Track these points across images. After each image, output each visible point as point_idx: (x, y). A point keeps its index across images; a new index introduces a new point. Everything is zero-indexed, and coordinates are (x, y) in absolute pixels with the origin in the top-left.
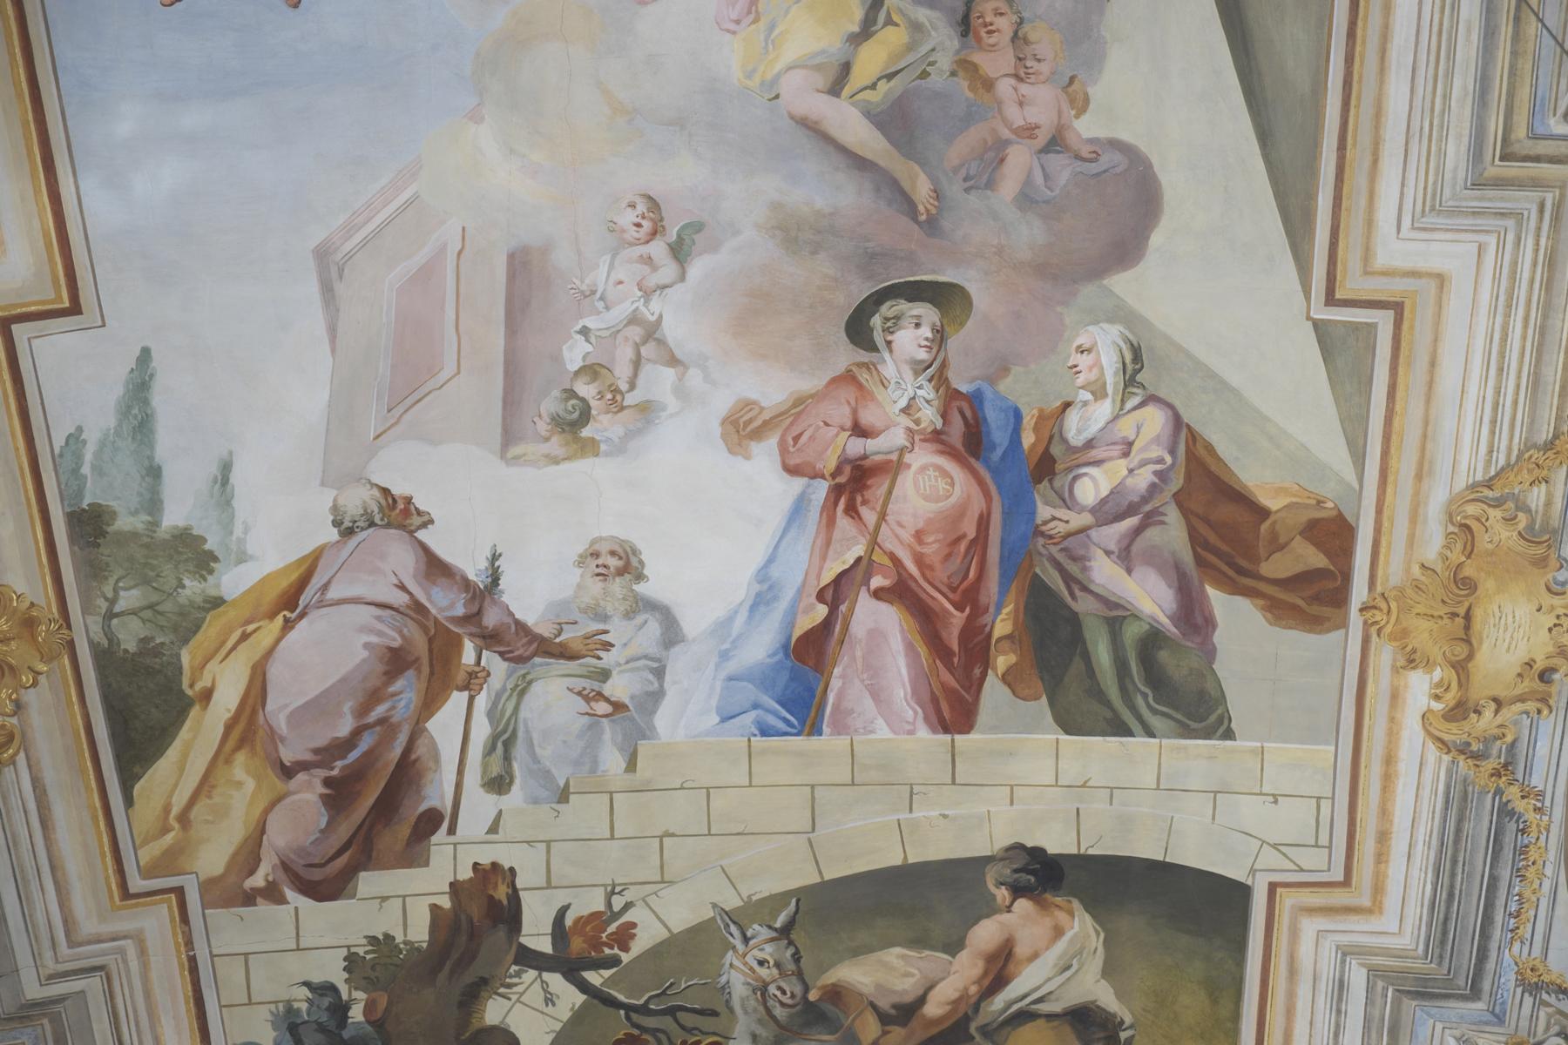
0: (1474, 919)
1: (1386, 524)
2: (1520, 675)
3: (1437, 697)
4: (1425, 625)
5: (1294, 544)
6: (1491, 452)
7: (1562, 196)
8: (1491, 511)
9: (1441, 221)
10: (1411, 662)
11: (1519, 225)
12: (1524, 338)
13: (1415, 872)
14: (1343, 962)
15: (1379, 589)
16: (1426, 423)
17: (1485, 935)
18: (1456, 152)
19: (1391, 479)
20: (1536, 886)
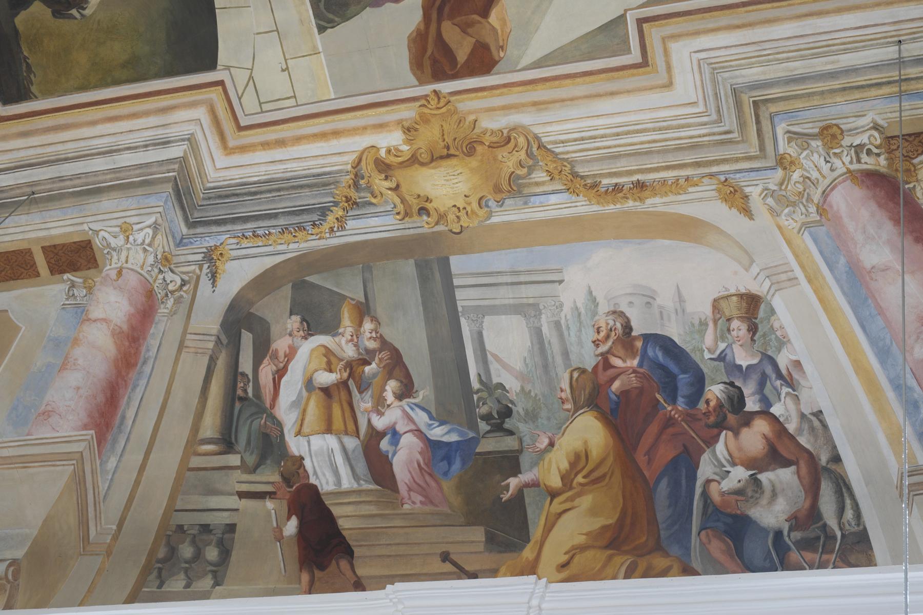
0: (242, 211)
1: (498, 92)
2: (419, 196)
3: (389, 151)
4: (436, 132)
5: (469, 39)
6: (563, 142)
7: (738, 142)
8: (524, 152)
9: (707, 76)
10: (408, 130)
11: (715, 122)
12: (642, 143)
13: (263, 168)
14: (183, 140)
15: (453, 99)
16: (572, 99)
17: (234, 221)
18: (754, 74)
19: (529, 87)
20: (279, 241)
